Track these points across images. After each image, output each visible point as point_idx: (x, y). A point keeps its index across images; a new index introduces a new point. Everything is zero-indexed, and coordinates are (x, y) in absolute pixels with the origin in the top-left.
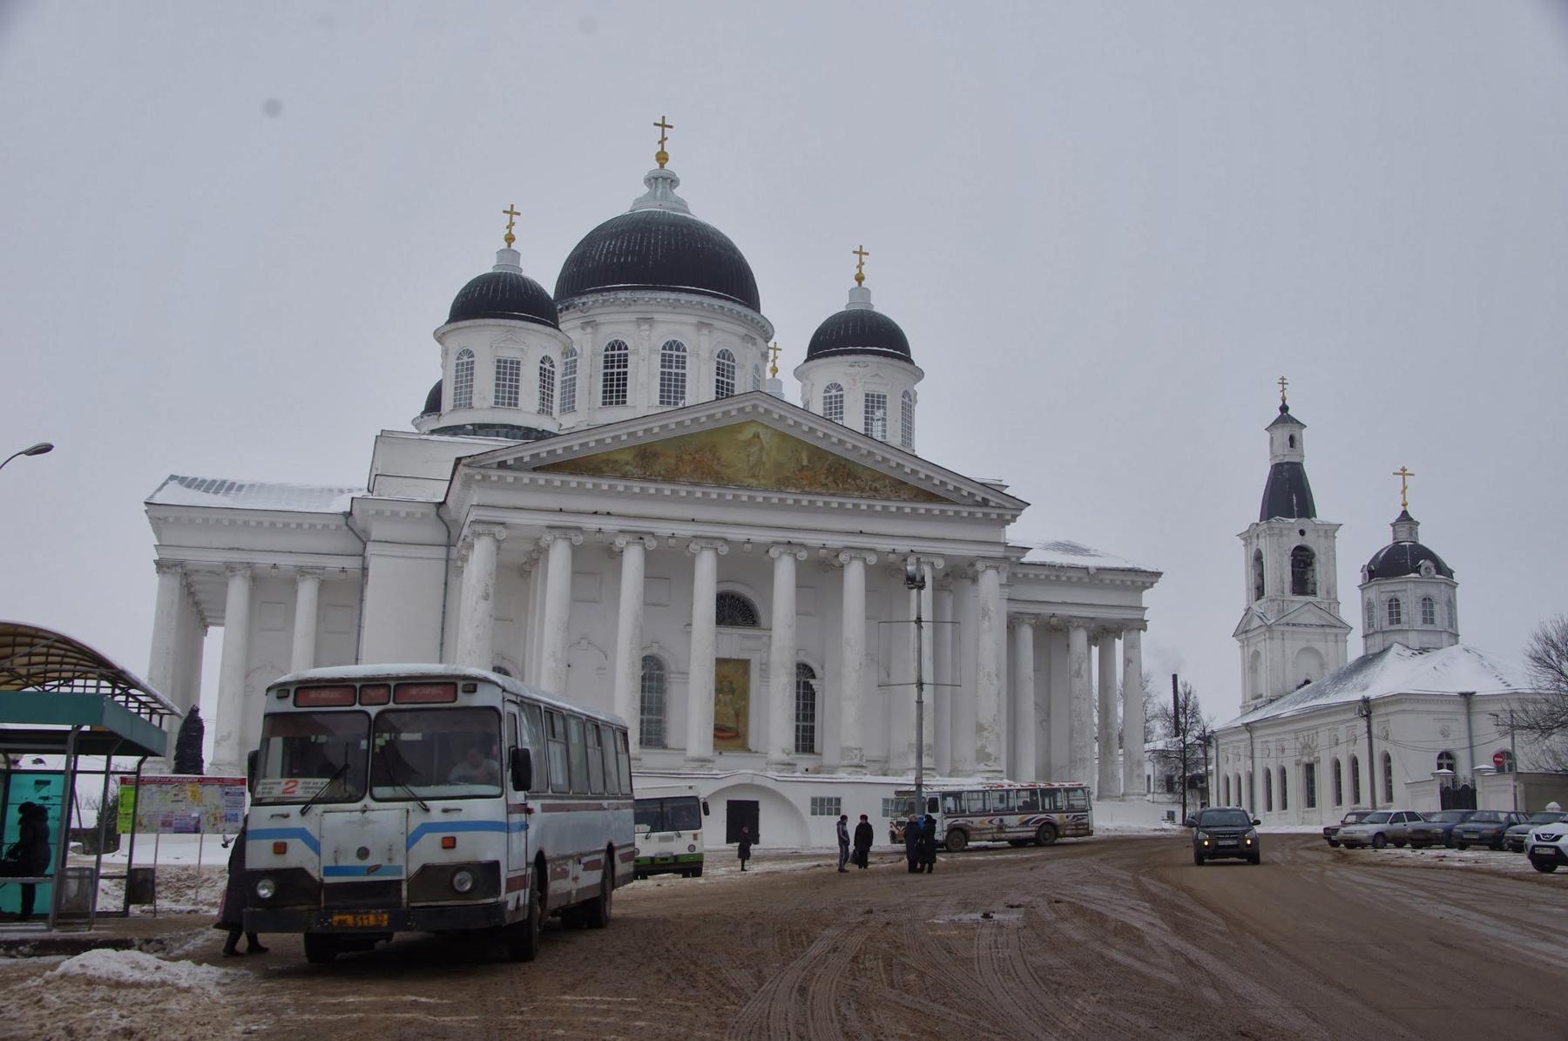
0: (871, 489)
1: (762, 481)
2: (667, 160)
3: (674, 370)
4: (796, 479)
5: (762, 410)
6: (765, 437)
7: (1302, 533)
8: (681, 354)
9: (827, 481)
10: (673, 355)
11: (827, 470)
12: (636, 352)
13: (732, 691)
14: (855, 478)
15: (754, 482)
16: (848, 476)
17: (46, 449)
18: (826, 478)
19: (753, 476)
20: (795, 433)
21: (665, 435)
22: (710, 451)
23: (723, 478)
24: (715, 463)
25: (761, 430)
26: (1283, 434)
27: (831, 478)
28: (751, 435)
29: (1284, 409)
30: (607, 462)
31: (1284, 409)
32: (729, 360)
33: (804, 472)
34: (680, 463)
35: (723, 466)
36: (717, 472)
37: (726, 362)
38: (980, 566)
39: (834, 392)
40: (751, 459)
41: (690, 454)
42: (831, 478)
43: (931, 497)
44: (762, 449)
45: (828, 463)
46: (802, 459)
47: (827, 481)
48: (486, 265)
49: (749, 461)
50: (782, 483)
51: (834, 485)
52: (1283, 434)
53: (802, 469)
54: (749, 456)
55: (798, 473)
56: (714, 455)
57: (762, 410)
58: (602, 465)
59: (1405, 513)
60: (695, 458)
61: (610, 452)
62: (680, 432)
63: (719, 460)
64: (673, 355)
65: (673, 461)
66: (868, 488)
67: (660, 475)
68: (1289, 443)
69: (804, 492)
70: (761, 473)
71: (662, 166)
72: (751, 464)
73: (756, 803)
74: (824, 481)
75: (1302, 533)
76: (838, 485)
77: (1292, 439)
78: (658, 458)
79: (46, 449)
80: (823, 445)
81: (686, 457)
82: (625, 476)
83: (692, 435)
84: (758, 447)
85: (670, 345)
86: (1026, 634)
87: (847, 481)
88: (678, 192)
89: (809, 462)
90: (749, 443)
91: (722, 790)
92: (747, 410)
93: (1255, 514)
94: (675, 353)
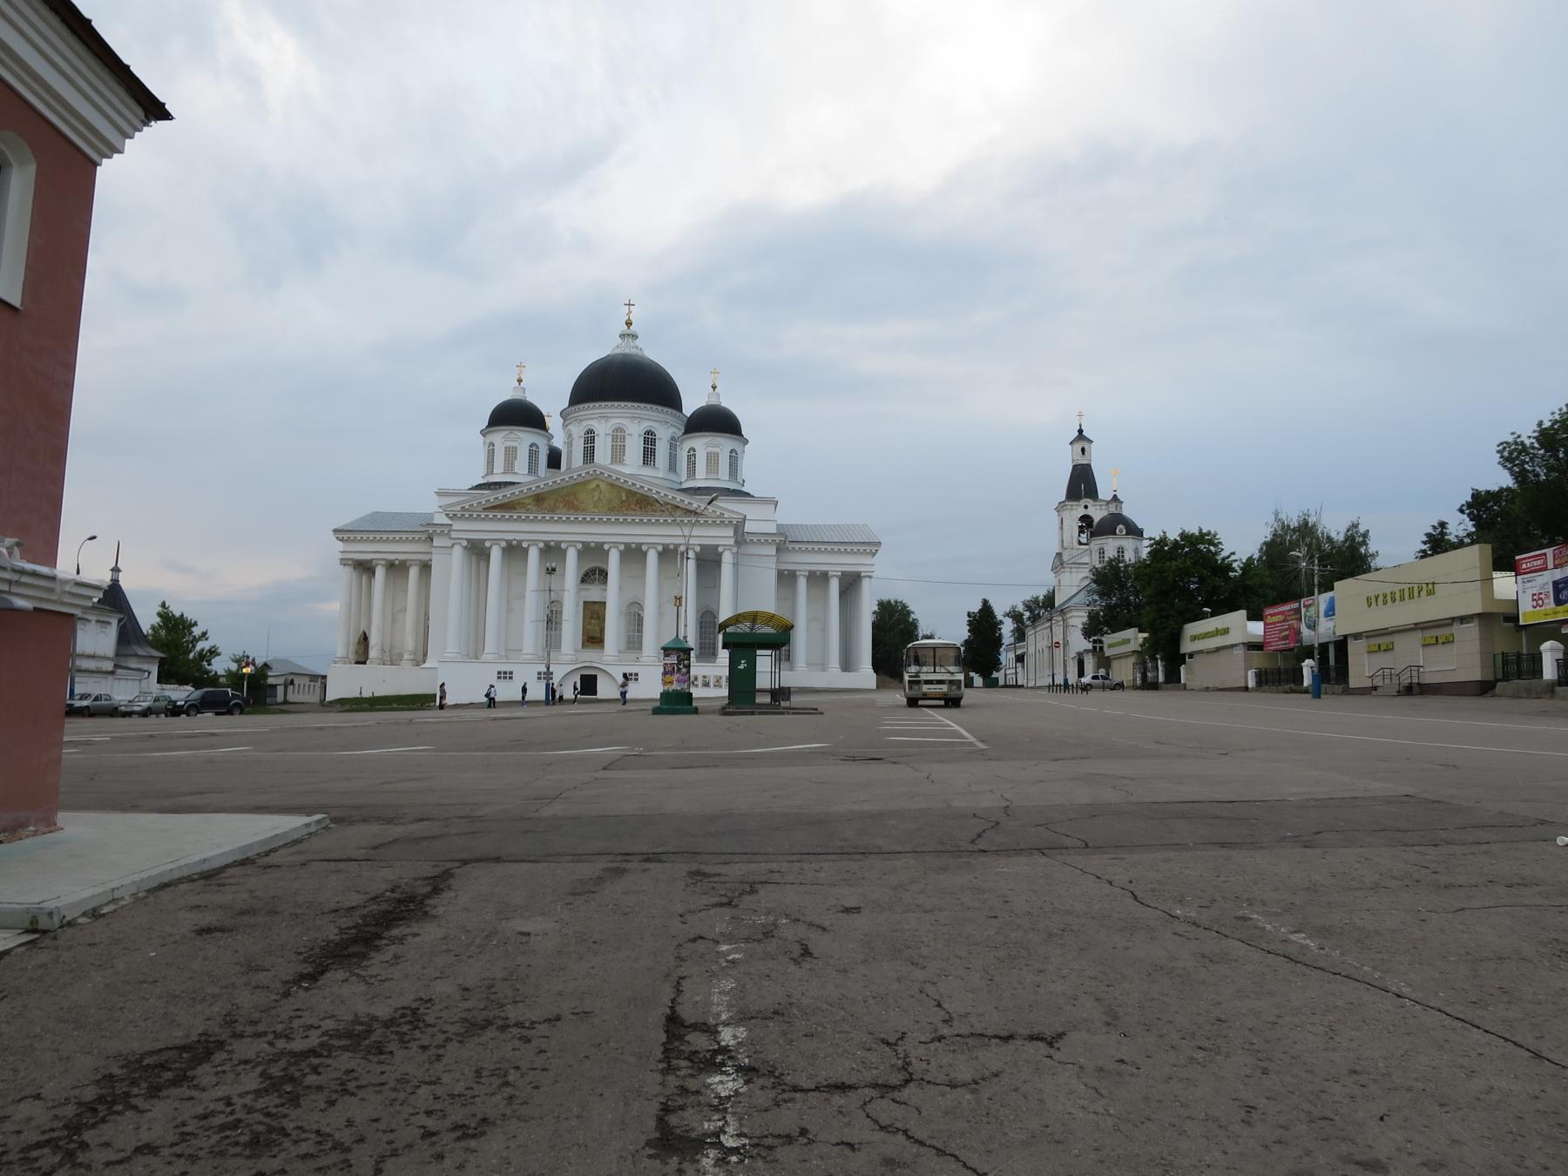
2: (631, 324)
3: (619, 443)
5: (598, 473)
6: (603, 486)
7: (1086, 507)
10: (618, 436)
12: (598, 435)
13: (598, 618)
14: (651, 505)
15: (596, 510)
17: (94, 538)
19: (595, 507)
20: (617, 483)
21: (547, 489)
25: (601, 484)
26: (1078, 447)
29: (1080, 431)
30: (519, 504)
31: (1080, 431)
33: (624, 504)
36: (576, 506)
38: (720, 549)
39: (692, 453)
44: (601, 492)
48: (506, 394)
50: (612, 510)
52: (1078, 447)
53: (622, 502)
57: (598, 473)
59: (1115, 496)
61: (519, 499)
62: (555, 487)
64: (618, 436)
67: (546, 509)
68: (1081, 453)
69: (627, 515)
71: (629, 328)
75: (1086, 507)
77: (1083, 450)
79: (94, 538)
80: (633, 489)
81: (559, 499)
82: (528, 510)
83: (563, 488)
84: (598, 492)
85: (617, 430)
86: (802, 583)
88: (637, 342)
89: (627, 497)
90: (594, 490)
91: (572, 671)
92: (591, 472)
93: (1062, 495)
94: (619, 434)
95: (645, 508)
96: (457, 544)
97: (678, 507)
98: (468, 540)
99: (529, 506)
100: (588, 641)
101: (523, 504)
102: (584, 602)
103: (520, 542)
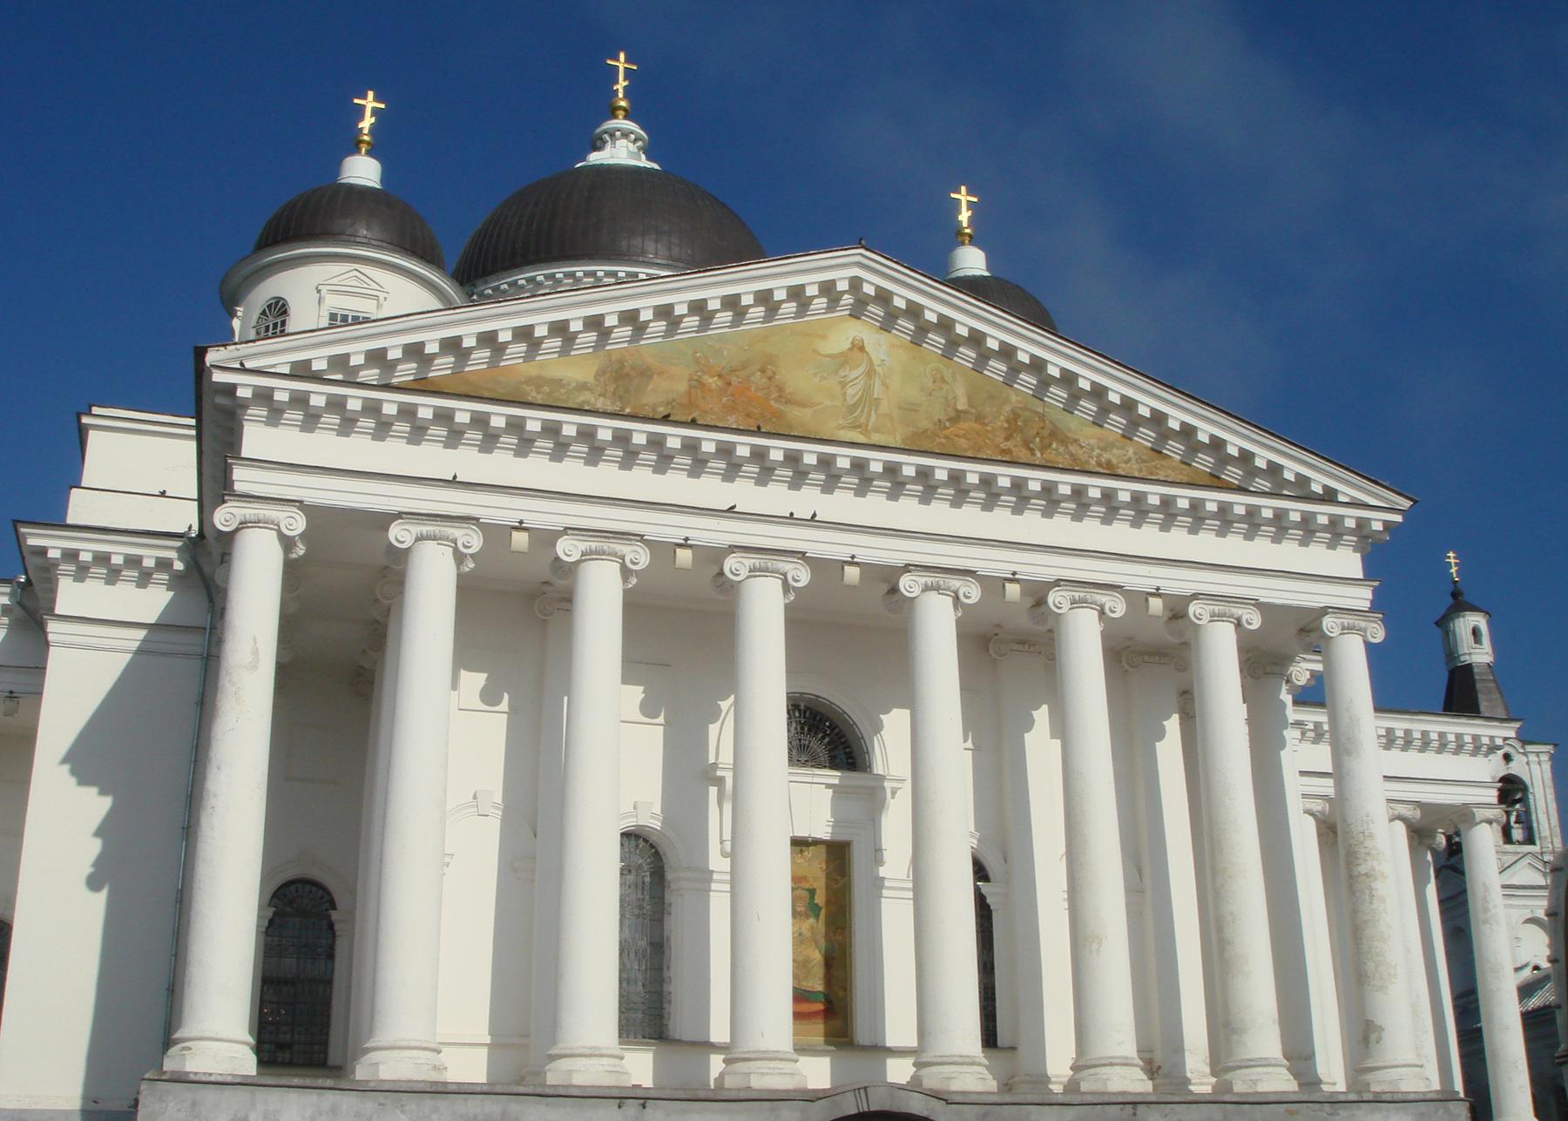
4: (946, 437)
9: (1009, 444)
11: (1008, 421)
18: (1007, 439)
22: (763, 371)
24: (775, 395)
27: (1018, 438)
35: (788, 402)
40: (850, 391)
41: (720, 376)
42: (1018, 438)
44: (870, 373)
45: (1008, 408)
46: (955, 398)
47: (1009, 444)
49: (844, 394)
53: (958, 417)
54: (843, 385)
55: (947, 424)
56: (770, 379)
58: (528, 389)
60: (729, 384)
63: (780, 389)
65: (682, 387)
66: (1093, 463)
70: (873, 418)
72: (850, 402)
78: (651, 377)
84: (861, 370)
87: (1050, 444)
89: (970, 405)
90: (843, 360)
95: (1043, 448)
96: (257, 523)
98: (314, 513)
103: (545, 538)
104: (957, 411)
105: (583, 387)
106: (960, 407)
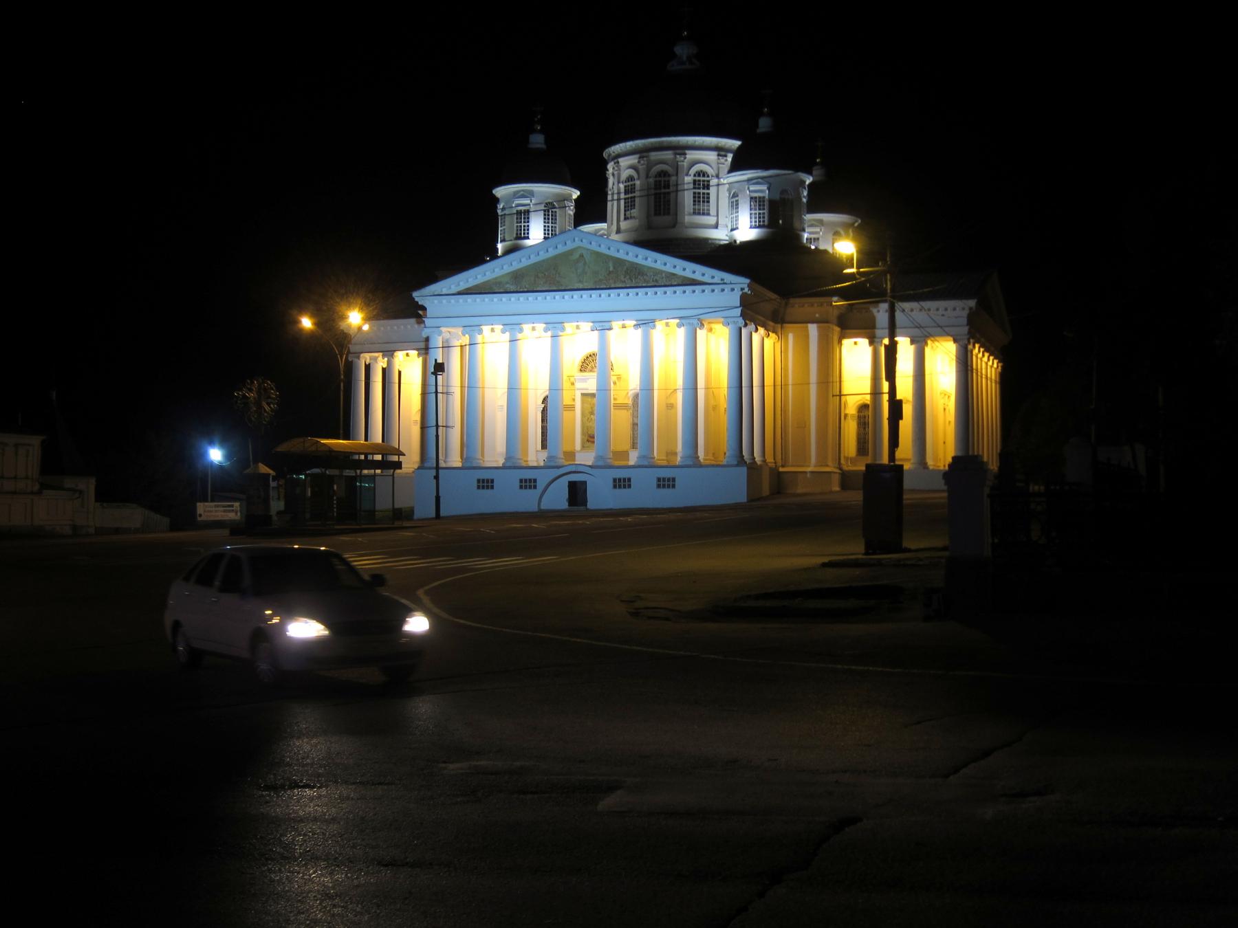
0: (653, 281)
1: (585, 284)
6: (587, 257)
8: (666, 179)
16: (639, 274)
18: (625, 277)
19: (580, 281)
22: (554, 269)
23: (562, 285)
24: (557, 275)
28: (578, 256)
32: (704, 176)
34: (537, 279)
36: (558, 282)
37: (702, 178)
40: (578, 271)
41: (543, 273)
42: (628, 277)
43: (694, 283)
44: (585, 263)
46: (609, 267)
51: (630, 281)
53: (610, 272)
61: (496, 278)
63: (559, 274)
73: (585, 483)
74: (623, 279)
76: (632, 280)
81: (540, 275)
89: (614, 268)
90: (577, 261)
95: (635, 278)
97: (674, 274)
99: (508, 286)
100: (588, 441)
101: (500, 283)
102: (582, 394)
104: (609, 271)
105: (507, 283)
106: (611, 269)
